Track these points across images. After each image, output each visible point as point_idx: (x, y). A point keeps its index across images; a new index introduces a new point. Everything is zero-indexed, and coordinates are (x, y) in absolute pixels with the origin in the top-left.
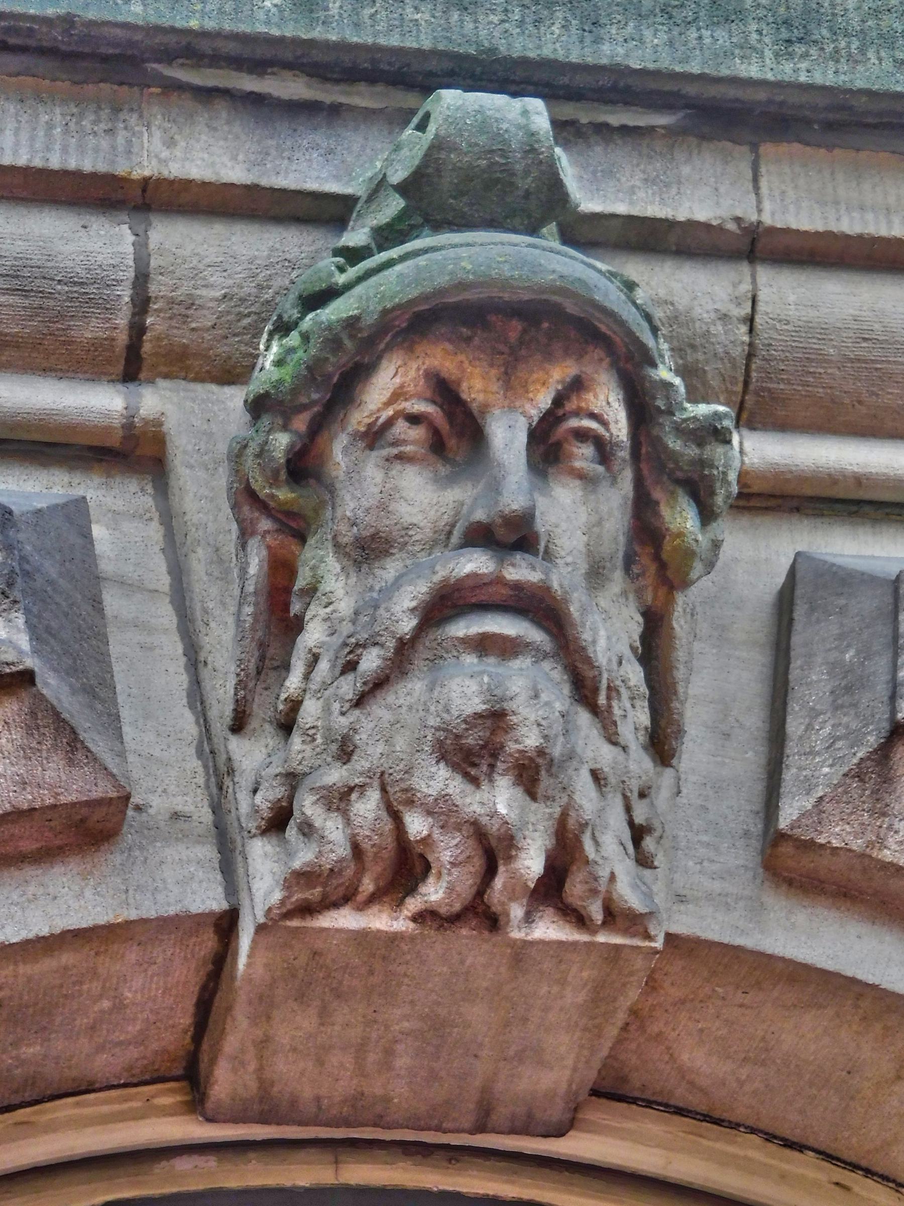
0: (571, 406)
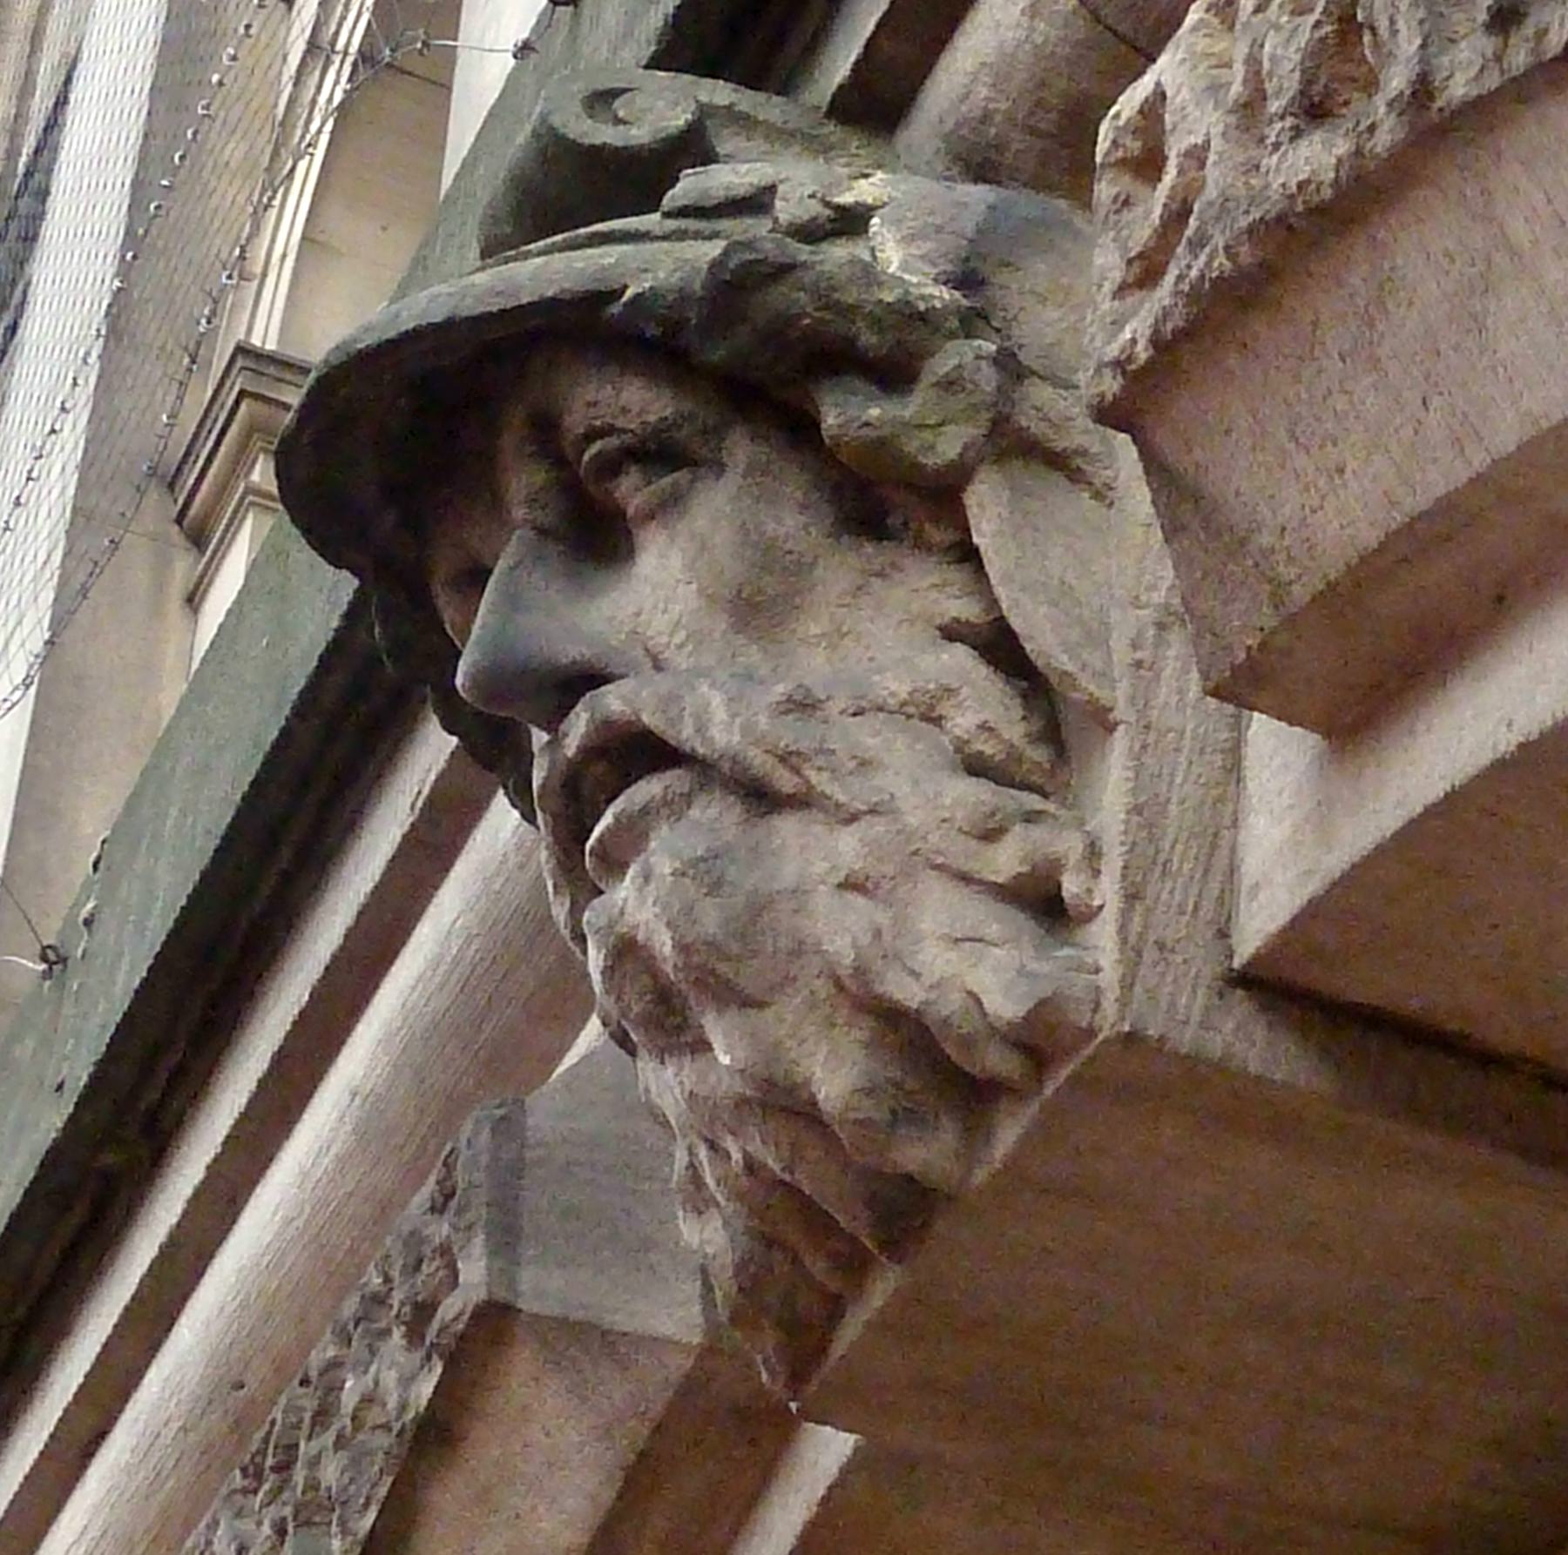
0: (570, 453)
